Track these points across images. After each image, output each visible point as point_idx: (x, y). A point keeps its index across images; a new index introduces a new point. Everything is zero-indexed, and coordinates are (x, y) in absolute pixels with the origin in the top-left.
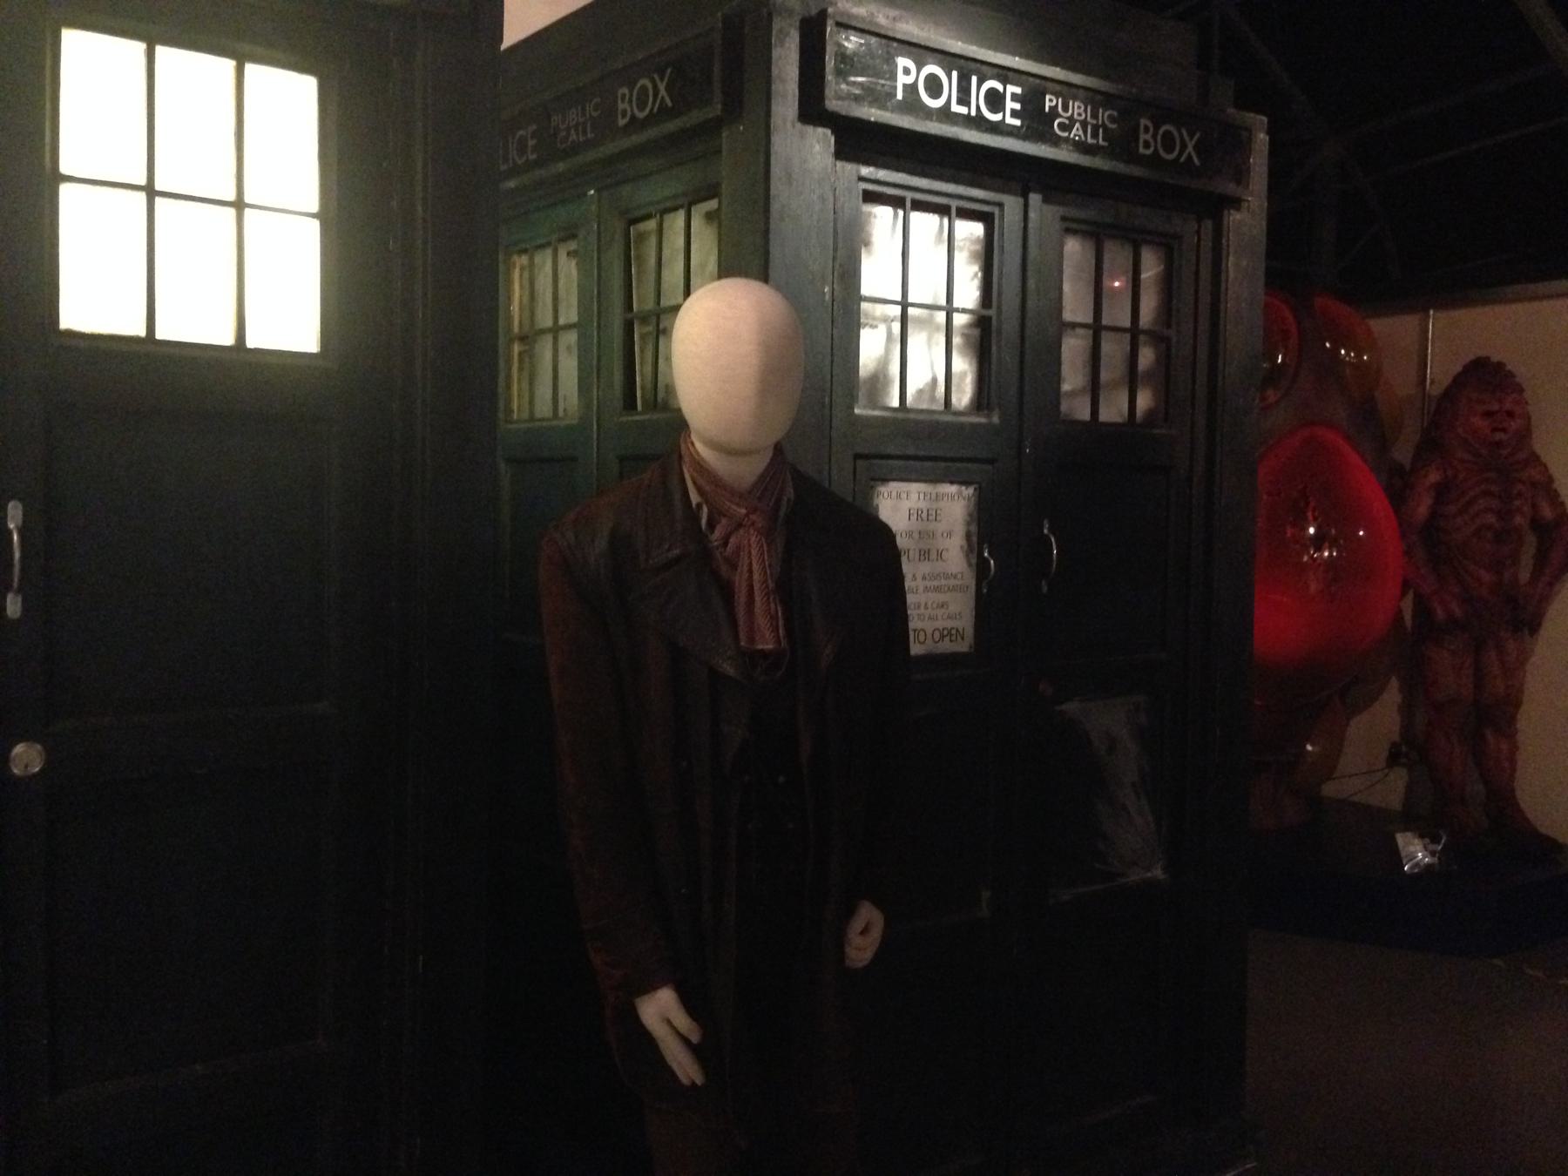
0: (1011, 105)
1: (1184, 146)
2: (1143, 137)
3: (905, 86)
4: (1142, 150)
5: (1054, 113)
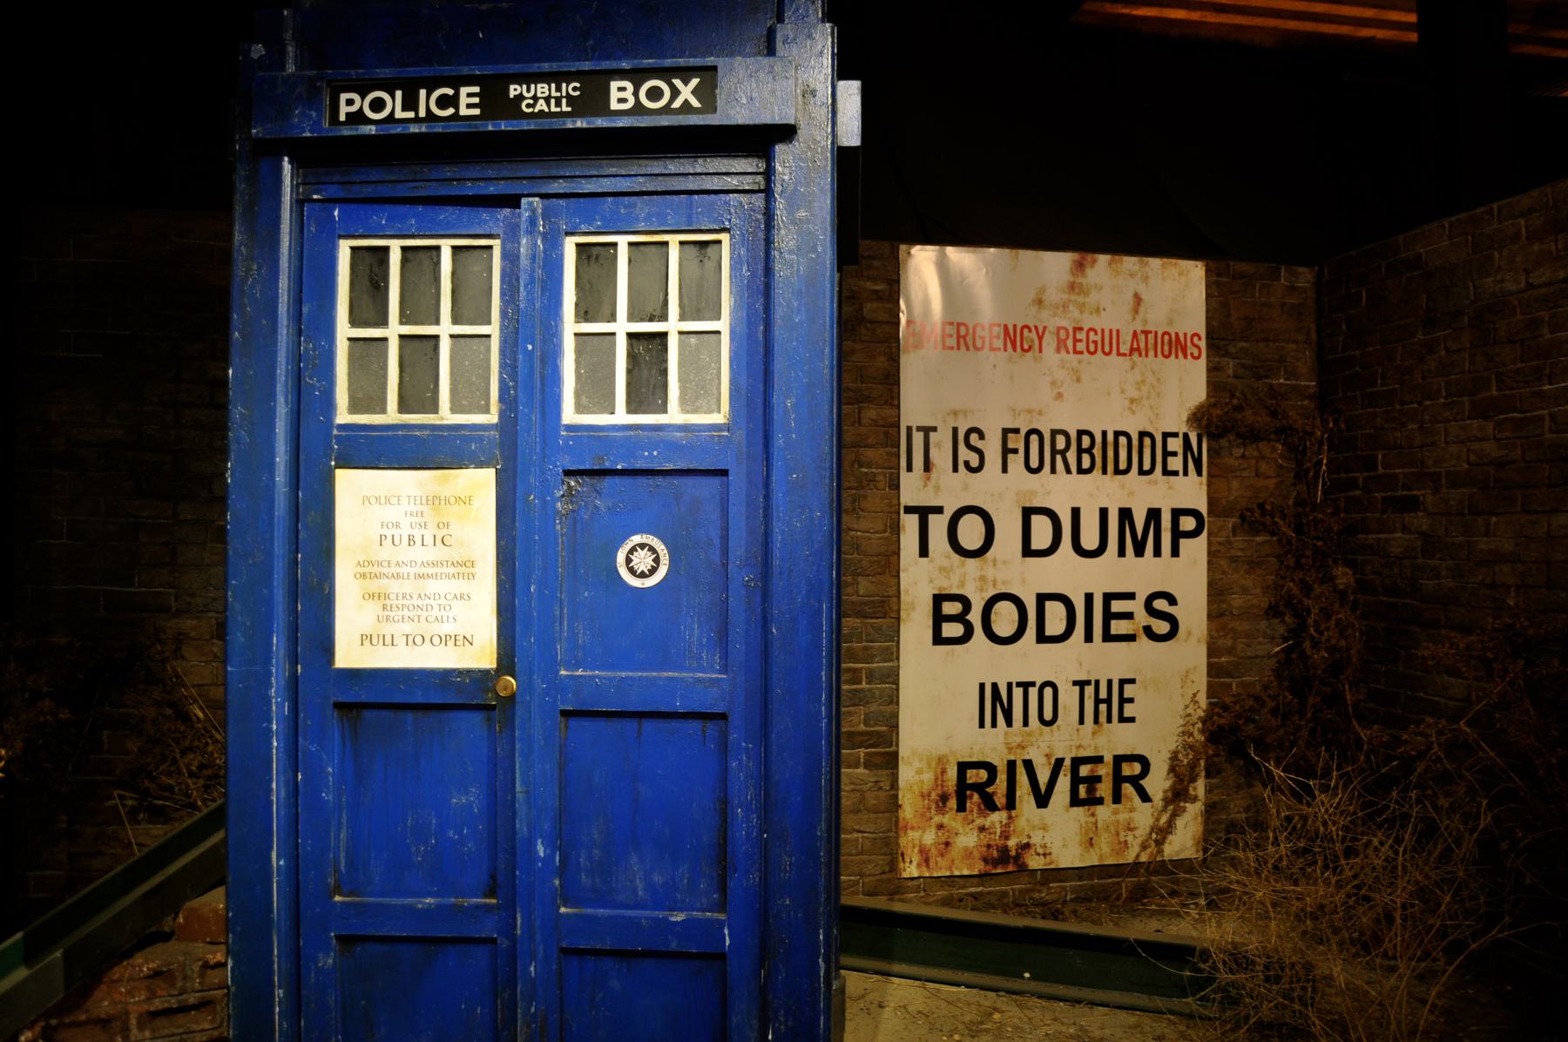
0: (464, 100)
1: (675, 93)
2: (614, 95)
4: (614, 106)
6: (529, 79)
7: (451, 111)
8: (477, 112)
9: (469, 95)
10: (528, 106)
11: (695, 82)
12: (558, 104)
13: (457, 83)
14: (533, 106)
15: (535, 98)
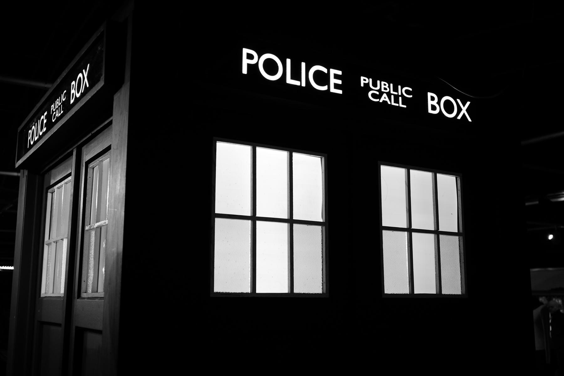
0: (333, 81)
1: (460, 110)
2: (430, 103)
3: (249, 65)
4: (430, 111)
7: (325, 88)
8: (340, 92)
9: (336, 76)
10: (374, 95)
12: (396, 101)
14: (379, 97)
15: (381, 93)
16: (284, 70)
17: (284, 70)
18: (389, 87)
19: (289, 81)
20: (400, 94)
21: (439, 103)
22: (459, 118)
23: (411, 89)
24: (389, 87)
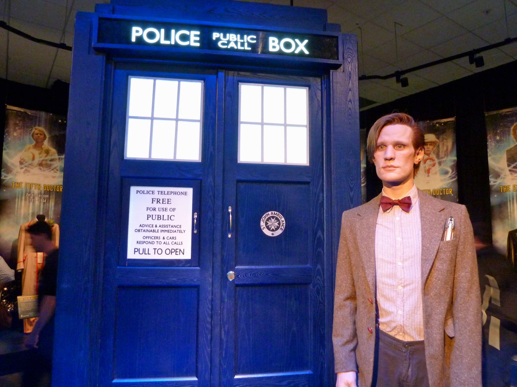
2: (271, 44)
5: (218, 39)
6: (225, 30)
9: (196, 36)
11: (306, 41)
12: (242, 44)
13: (190, 27)
15: (229, 42)
16: (160, 36)
17: (160, 36)
18: (237, 37)
19: (163, 42)
20: (245, 41)
21: (279, 44)
22: (297, 52)
23: (255, 37)
24: (237, 37)
